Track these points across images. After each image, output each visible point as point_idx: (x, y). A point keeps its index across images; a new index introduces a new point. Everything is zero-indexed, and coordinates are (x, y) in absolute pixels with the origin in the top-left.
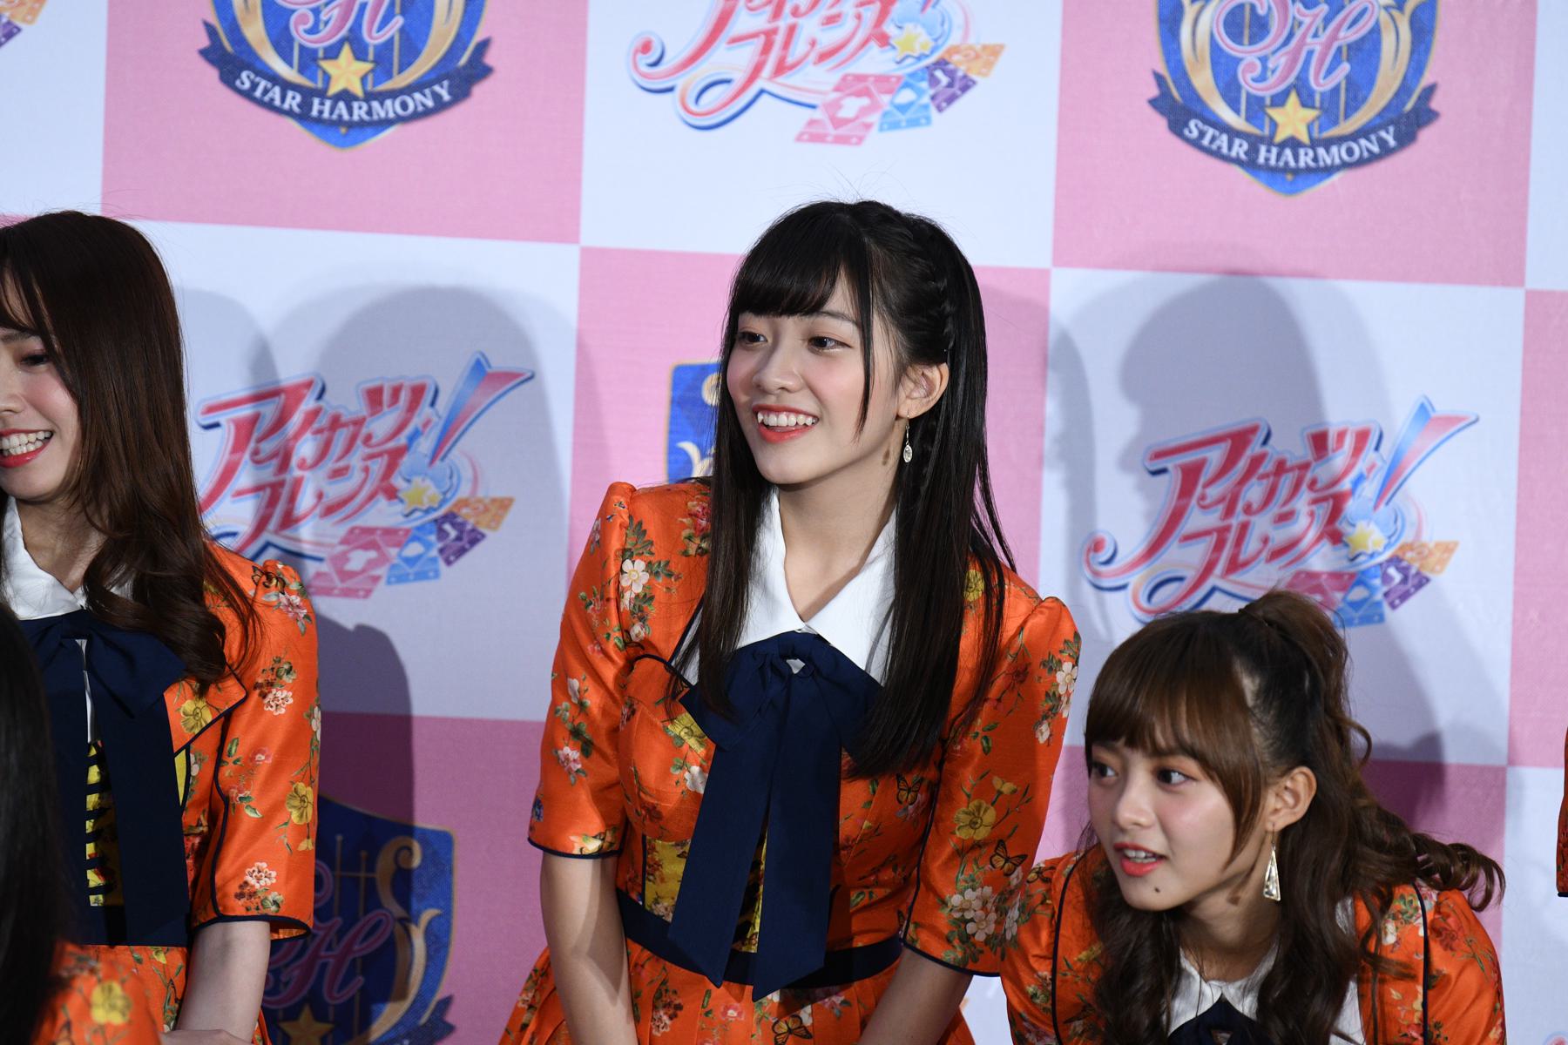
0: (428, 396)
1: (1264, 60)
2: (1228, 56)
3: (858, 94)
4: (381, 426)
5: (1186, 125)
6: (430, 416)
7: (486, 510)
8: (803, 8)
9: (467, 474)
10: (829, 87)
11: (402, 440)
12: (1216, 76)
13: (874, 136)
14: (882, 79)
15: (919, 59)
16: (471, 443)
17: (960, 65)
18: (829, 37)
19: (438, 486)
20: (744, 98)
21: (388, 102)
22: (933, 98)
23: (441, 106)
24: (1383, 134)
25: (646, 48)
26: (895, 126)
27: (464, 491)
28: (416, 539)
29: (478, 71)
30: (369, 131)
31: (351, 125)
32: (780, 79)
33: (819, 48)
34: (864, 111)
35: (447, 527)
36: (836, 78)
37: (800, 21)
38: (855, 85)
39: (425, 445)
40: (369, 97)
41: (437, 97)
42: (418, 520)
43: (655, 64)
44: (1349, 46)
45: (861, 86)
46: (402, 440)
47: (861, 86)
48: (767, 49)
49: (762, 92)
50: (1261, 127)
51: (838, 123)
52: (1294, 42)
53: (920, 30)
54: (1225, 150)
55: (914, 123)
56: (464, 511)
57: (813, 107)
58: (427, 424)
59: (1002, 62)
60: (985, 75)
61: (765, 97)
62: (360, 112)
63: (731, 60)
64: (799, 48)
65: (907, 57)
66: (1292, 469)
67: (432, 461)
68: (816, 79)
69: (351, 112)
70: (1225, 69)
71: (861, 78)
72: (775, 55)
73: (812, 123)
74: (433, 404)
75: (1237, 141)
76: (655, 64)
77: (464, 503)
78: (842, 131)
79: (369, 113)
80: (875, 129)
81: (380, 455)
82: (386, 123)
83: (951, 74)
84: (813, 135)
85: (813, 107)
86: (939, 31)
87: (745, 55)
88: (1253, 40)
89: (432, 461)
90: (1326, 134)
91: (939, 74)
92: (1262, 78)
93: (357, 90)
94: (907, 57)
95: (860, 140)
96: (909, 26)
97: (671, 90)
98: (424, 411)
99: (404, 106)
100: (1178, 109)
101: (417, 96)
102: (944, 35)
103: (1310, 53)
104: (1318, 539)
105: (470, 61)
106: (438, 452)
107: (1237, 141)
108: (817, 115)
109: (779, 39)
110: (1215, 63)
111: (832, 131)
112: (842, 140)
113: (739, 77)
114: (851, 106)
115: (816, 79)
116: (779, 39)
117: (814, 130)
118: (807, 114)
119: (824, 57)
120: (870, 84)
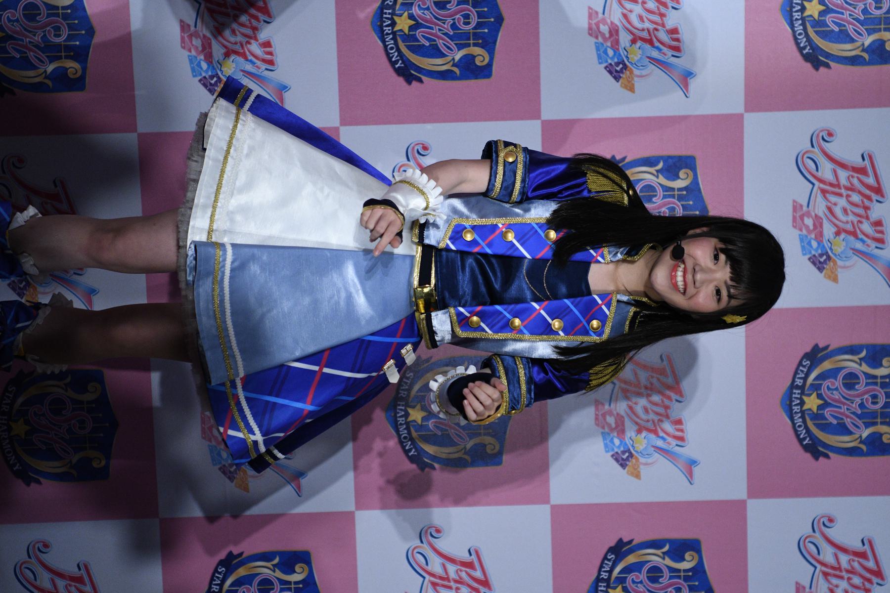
1: (837, 389)
3: (814, 225)
4: (663, 35)
7: (629, 82)
8: (850, 199)
9: (644, 73)
11: (657, 44)
12: (830, 370)
14: (821, 234)
15: (831, 249)
16: (657, 73)
18: (838, 211)
19: (638, 61)
21: (801, 27)
25: (830, 134)
26: (802, 240)
27: (636, 72)
30: (789, 21)
31: (791, 11)
33: (833, 207)
34: (807, 227)
35: (621, 66)
36: (821, 214)
37: (845, 198)
38: (818, 223)
39: (655, 54)
40: (803, 19)
46: (657, 44)
48: (831, 185)
53: (843, 248)
55: (803, 248)
56: (628, 72)
59: (830, 283)
60: (825, 276)
61: (811, 186)
62: (796, 15)
63: (826, 170)
64: (833, 199)
67: (648, 57)
68: (820, 207)
69: (796, 11)
72: (830, 189)
73: (801, 206)
77: (631, 72)
79: (797, 19)
80: (800, 233)
81: (650, 35)
82: (792, 27)
84: (796, 207)
86: (843, 256)
87: (828, 176)
89: (648, 57)
90: (807, 417)
93: (806, 13)
96: (844, 243)
98: (670, 53)
99: (800, 34)
100: (815, 356)
102: (841, 258)
108: (805, 208)
109: (836, 190)
112: (794, 219)
113: (819, 174)
114: (809, 222)
116: (836, 190)
118: (805, 204)
119: (830, 209)
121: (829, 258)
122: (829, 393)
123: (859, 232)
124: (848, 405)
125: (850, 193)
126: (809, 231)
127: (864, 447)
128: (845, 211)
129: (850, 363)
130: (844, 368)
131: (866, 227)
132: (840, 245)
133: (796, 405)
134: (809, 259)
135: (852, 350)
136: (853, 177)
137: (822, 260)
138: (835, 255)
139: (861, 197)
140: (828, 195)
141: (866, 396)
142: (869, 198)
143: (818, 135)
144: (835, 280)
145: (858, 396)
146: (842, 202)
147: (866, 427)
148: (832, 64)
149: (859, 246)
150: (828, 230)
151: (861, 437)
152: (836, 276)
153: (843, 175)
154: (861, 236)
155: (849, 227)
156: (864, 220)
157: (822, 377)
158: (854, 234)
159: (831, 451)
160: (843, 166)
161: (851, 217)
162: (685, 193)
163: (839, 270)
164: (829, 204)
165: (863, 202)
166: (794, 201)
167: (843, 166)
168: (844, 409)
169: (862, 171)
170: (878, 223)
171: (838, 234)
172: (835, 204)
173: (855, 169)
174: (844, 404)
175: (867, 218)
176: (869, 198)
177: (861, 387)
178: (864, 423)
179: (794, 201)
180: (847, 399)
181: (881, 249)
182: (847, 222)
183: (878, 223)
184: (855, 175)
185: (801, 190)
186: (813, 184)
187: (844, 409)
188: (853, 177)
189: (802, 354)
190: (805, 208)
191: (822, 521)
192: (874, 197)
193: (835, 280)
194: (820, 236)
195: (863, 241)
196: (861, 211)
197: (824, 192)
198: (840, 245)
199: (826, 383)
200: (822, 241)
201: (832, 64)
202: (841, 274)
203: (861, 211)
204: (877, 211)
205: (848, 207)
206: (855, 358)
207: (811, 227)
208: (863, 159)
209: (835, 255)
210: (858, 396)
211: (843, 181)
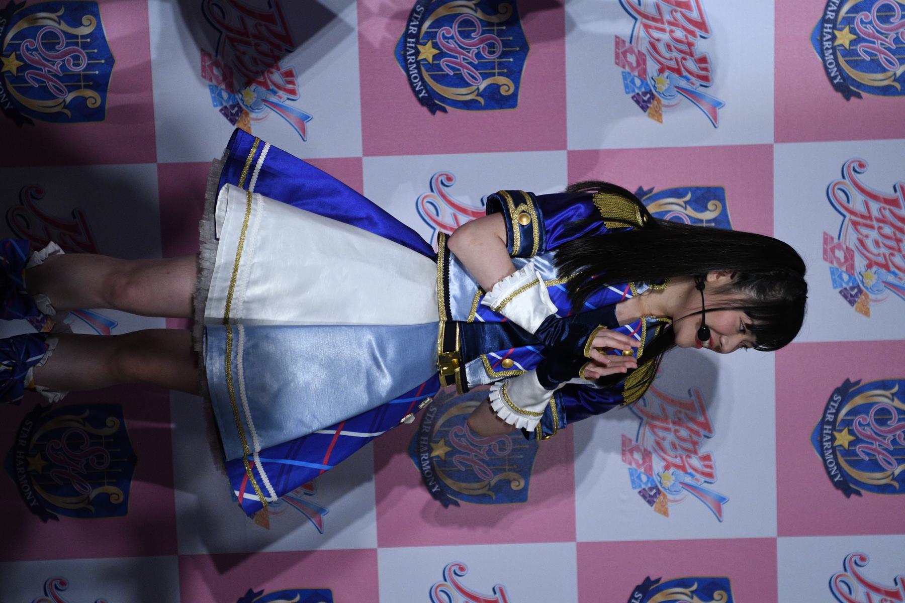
92: (445, 37)
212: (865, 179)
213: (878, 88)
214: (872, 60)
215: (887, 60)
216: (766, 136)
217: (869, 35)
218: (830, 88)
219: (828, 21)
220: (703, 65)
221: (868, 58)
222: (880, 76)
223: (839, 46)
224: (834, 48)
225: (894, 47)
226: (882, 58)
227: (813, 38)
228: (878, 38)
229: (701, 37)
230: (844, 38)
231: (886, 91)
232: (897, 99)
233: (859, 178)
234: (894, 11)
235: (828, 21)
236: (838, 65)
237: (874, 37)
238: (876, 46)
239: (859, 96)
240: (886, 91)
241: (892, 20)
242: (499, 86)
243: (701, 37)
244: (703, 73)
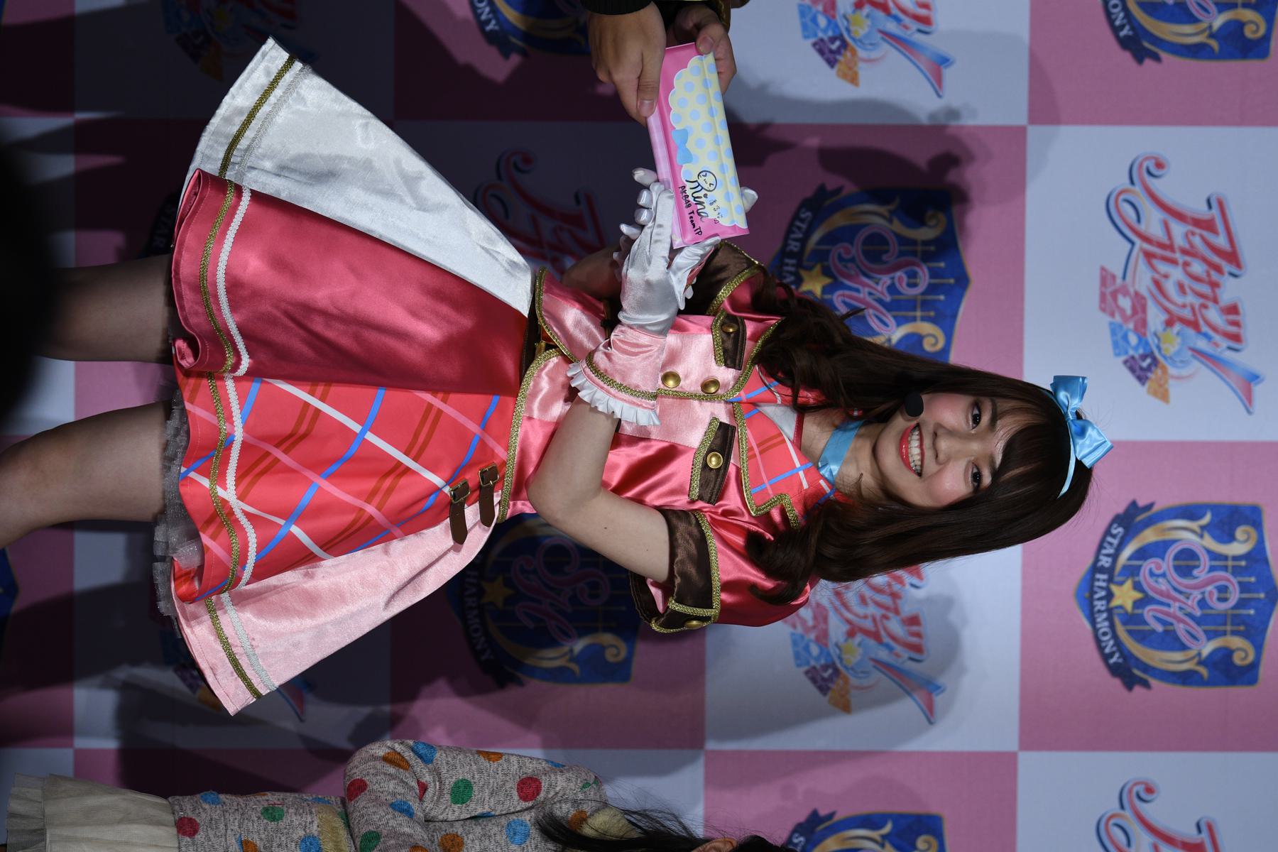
0: (923, 27)
1: (1164, 575)
2: (1165, 552)
5: (1120, 525)
6: (912, 31)
9: (874, 55)
10: (1137, 287)
13: (1106, 319)
17: (1154, 375)
18: (1170, 287)
20: (1130, 232)
22: (1133, 357)
23: (1116, 30)
24: (1117, 655)
26: (1113, 333)
27: (861, 53)
28: (829, 22)
29: (1140, 55)
32: (1141, 256)
33: (1162, 280)
34: (1122, 311)
36: (1144, 292)
38: (1139, 305)
41: (1122, 27)
42: (842, 24)
43: (1149, 173)
44: (1174, 632)
45: (1139, 309)
47: (1139, 309)
49: (1133, 243)
50: (1120, 574)
51: (1114, 295)
52: (1174, 593)
54: (1104, 552)
57: (1124, 277)
58: (906, 27)
59: (1157, 402)
60: (1149, 391)
61: (1128, 246)
63: (1153, 222)
65: (1159, 339)
66: (895, 603)
68: (1142, 280)
70: (1157, 550)
71: (1144, 309)
72: (1157, 252)
73: (1114, 277)
74: (920, 31)
75: (1110, 560)
76: (1149, 173)
78: (1109, 298)
83: (1149, 369)
85: (1124, 277)
86: (1177, 359)
87: (1156, 231)
88: (1177, 568)
91: (1148, 361)
94: (1159, 339)
95: (1103, 310)
96: (1179, 340)
97: (1132, 182)
101: (1122, 15)
102: (1174, 363)
103: (1169, 605)
104: (848, 622)
105: (1145, 49)
106: (887, 35)
107: (1110, 560)
108: (1119, 281)
109: (1168, 254)
110: (1156, 544)
111: (1109, 290)
112: (1103, 297)
114: (1125, 303)
115: (1142, 280)
116: (1168, 254)
117: (1109, 281)
118: (1119, 274)
119: (1157, 284)
120: (1140, 315)
121: (1155, 362)
122: (1151, 581)
123: (1201, 322)
124: (1181, 599)
125: (1188, 259)
126: (1126, 319)
127: (1204, 671)
128: (1181, 288)
129: (1186, 534)
130: (1174, 541)
131: (1213, 315)
132: (1173, 343)
133: (1100, 599)
134: (1125, 362)
135: (1190, 512)
136: (1193, 234)
137: (1145, 364)
138: (1165, 357)
139: (1205, 267)
140: (1155, 262)
141: (1210, 588)
142: (1218, 269)
143: (1141, 165)
144: (1164, 397)
145: (1195, 587)
146: (1177, 274)
147: (1209, 639)
148: (1163, 55)
149: (1202, 344)
150: (1155, 318)
151: (1199, 654)
152: (1167, 391)
153: (1178, 230)
154: (1205, 329)
155: (1187, 313)
156: (1210, 304)
157: (1142, 554)
158: (1194, 325)
159: (1154, 676)
160: (1180, 216)
161: (1190, 299)
162: (932, 248)
163: (1171, 382)
164: (1157, 276)
165: (1208, 275)
166: (1103, 269)
167: (1180, 216)
168: (1174, 608)
169: (1208, 225)
170: (1233, 310)
171: (1169, 323)
172: (1166, 276)
173: (1197, 223)
174: (1175, 600)
175: (1215, 301)
176: (1218, 269)
177: (1201, 573)
178: (1205, 631)
179: (1103, 269)
180: (1181, 592)
181: (1236, 350)
182: (1184, 306)
183: (1233, 310)
184: (1197, 231)
185: (1114, 252)
186: (1133, 243)
187: (1174, 608)
188: (1193, 234)
189: (1109, 517)
190: (1119, 281)
191: (1135, 790)
192: (1227, 267)
193: (1164, 397)
194: (1141, 326)
195: (1208, 338)
196: (1205, 289)
197: (1149, 256)
198: (1173, 343)
199: (1148, 565)
200: (1145, 334)
201: (1163, 55)
202: (1174, 388)
203: (1205, 289)
204: (1230, 290)
205: (1187, 282)
206: (1194, 525)
207: (1129, 312)
208: (1210, 206)
209: (1165, 357)
210: (1195, 587)
211: (1179, 241)
212: (1154, 811)
213: (1174, 674)
214: (1166, 632)
215: (1188, 632)
216: (1008, 740)
217: (1161, 593)
218: (1104, 671)
219: (1102, 570)
220: (915, 628)
221: (1160, 628)
222: (1178, 656)
223: (1118, 607)
224: (1110, 611)
225: (1198, 613)
226: (1180, 629)
227: (1078, 595)
228: (1175, 600)
229: (912, 585)
230: (1125, 596)
231: (1186, 678)
232: (1204, 691)
233: (1145, 809)
234: (1198, 559)
235: (1102, 570)
236: (1115, 636)
237: (1169, 596)
238: (1172, 610)
239: (1146, 684)
240: (1186, 678)
241: (1195, 572)
242: (603, 648)
243: (912, 585)
244: (914, 640)
